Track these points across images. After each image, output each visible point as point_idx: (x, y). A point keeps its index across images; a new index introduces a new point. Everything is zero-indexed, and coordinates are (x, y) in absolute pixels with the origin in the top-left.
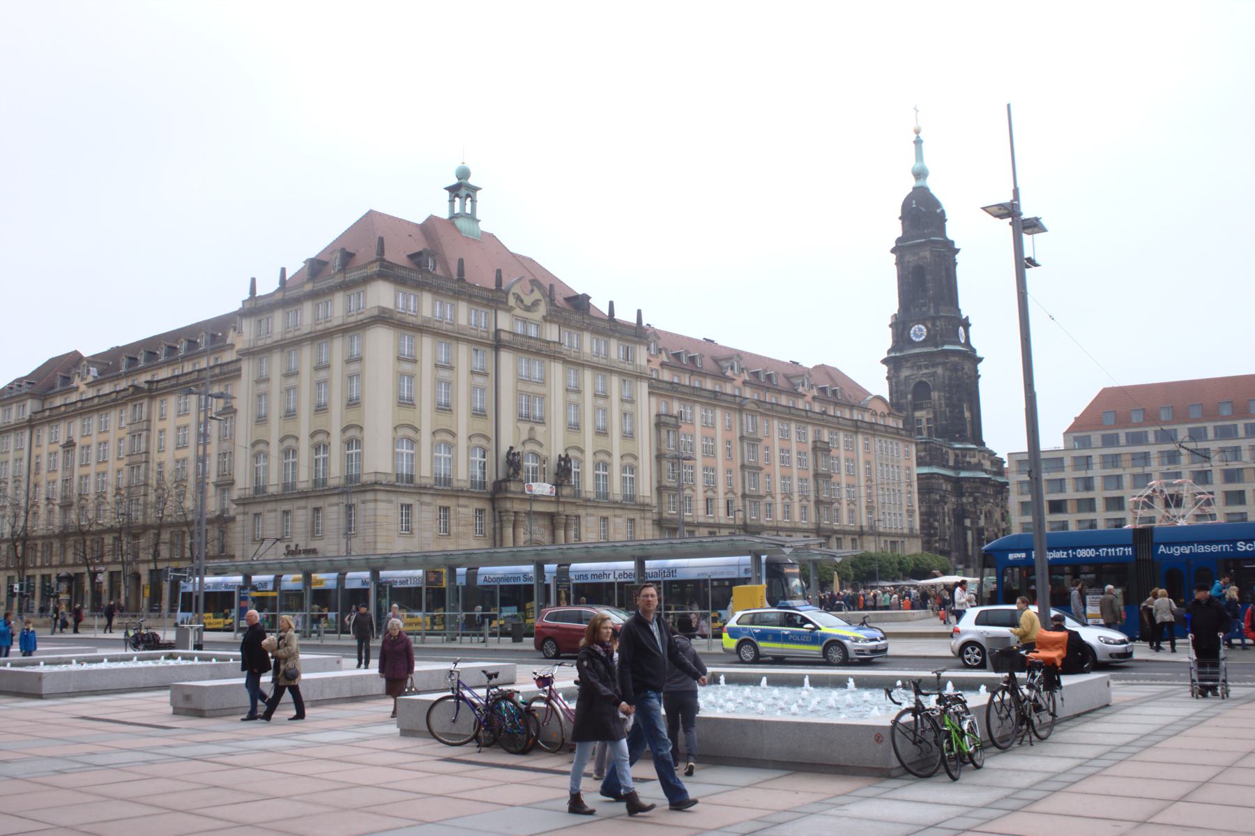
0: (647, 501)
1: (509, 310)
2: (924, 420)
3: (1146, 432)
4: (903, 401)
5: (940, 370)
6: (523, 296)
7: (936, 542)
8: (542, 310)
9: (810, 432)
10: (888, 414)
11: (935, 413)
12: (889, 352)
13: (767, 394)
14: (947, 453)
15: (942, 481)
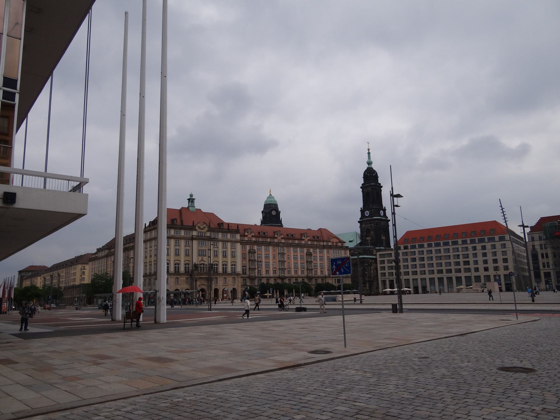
0: (239, 273)
1: (196, 230)
2: (369, 240)
3: (416, 245)
4: (363, 234)
5: (373, 225)
6: (200, 226)
7: (367, 278)
8: (206, 229)
9: (305, 250)
10: (339, 242)
11: (372, 238)
12: (360, 219)
13: (290, 241)
14: (373, 251)
15: (369, 259)
